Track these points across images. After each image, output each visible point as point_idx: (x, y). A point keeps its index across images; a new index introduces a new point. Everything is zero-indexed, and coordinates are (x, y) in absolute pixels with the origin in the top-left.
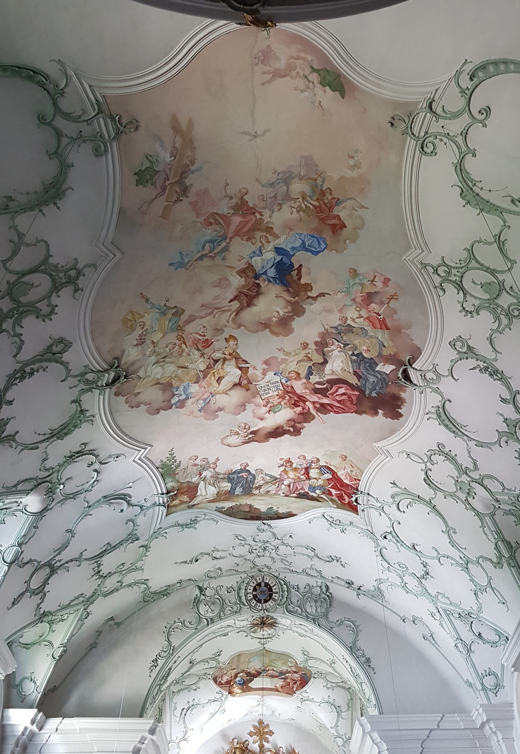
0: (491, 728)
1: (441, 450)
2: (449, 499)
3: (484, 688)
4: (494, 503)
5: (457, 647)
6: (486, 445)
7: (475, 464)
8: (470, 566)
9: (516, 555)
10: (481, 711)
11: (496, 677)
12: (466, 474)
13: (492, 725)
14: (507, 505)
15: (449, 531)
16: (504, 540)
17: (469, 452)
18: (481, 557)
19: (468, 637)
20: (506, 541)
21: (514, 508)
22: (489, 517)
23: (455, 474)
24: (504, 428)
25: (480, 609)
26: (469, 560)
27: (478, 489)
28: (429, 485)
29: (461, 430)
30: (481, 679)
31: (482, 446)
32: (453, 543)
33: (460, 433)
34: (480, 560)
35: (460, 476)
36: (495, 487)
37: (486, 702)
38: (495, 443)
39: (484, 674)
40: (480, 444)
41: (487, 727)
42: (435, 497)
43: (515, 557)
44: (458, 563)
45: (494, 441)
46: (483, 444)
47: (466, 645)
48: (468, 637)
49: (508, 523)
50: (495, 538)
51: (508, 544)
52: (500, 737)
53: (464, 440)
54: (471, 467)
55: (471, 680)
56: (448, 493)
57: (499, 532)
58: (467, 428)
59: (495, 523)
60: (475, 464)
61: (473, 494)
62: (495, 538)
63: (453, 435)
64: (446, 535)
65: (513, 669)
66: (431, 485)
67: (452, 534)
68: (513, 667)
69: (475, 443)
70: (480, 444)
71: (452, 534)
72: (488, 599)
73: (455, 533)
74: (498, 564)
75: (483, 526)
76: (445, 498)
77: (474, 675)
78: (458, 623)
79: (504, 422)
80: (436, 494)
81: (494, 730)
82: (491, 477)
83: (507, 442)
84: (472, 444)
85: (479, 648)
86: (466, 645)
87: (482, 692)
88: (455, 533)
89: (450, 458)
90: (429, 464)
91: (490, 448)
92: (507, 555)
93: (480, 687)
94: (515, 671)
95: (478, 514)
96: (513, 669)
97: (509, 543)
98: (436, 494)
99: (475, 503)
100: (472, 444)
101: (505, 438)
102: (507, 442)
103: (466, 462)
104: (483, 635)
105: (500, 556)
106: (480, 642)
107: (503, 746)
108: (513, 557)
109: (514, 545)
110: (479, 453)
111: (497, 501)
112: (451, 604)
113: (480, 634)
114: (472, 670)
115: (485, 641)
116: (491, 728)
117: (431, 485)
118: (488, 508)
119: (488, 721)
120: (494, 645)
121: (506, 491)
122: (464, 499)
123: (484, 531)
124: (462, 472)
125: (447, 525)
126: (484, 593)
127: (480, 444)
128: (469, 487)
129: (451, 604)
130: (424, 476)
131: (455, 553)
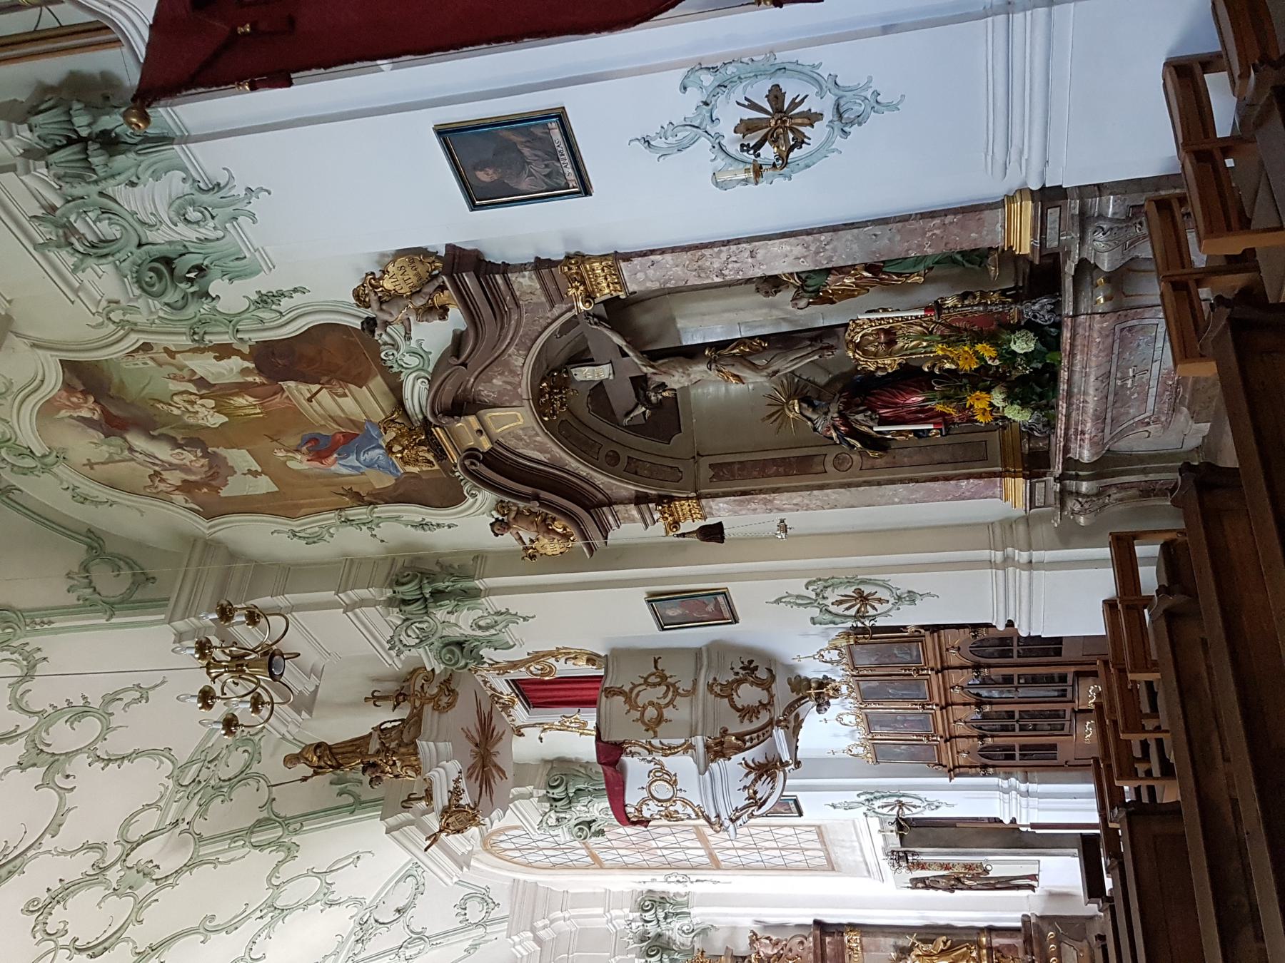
0: (545, 927)
1: (38, 910)
2: (145, 915)
3: (482, 924)
4: (177, 830)
5: (411, 958)
6: (59, 816)
7: (91, 848)
8: (279, 904)
9: (282, 815)
10: (516, 939)
11: (469, 897)
12: (105, 869)
13: (540, 924)
14: (190, 808)
15: (207, 929)
16: (251, 830)
17: (64, 853)
18: (269, 879)
19: (397, 935)
20: (254, 826)
21: (199, 796)
22: (201, 847)
23: (99, 891)
24: (36, 774)
25: (358, 902)
26: (269, 902)
27: (142, 854)
28: (106, 949)
29: (11, 857)
30: (467, 926)
31: (60, 825)
32: (231, 927)
33: (18, 862)
34: (275, 882)
35: (107, 884)
36: (150, 820)
37: (505, 926)
38: (61, 798)
39: (462, 918)
40: (54, 828)
41: (541, 933)
42: (134, 942)
43: (286, 818)
44: (269, 925)
45: (57, 799)
46: (57, 822)
47: (410, 942)
48: (397, 935)
49: (222, 815)
50: (243, 846)
51: (259, 824)
52: (558, 914)
53: (32, 858)
54: (94, 856)
55: (467, 945)
56: (134, 915)
57: (234, 836)
58: (11, 846)
59: (215, 839)
60: (91, 848)
61: (150, 865)
62: (243, 846)
63: (16, 876)
64: (213, 936)
65: (465, 869)
66: (106, 945)
67: (214, 923)
68: (462, 869)
69: (48, 836)
70: (54, 828)
71: (214, 923)
72: (344, 884)
73: (213, 917)
74: (291, 851)
75: (215, 863)
76: (141, 922)
77: (460, 937)
78: (372, 947)
79: (23, 770)
80: (127, 940)
81: (547, 922)
82: (127, 823)
83: (68, 776)
84: (48, 842)
85: (421, 918)
86: (410, 942)
87: (489, 929)
88: (213, 917)
89: (61, 895)
90: (62, 941)
91: (69, 810)
92: (279, 832)
93: (481, 931)
94: (468, 866)
95: (189, 866)
96: (465, 869)
97: (259, 824)
98: (127, 940)
99: (168, 866)
100: (48, 842)
101: (59, 779)
102: (68, 776)
103: (84, 863)
104: (401, 905)
105: (278, 844)
106: (410, 912)
107: (574, 912)
108: (284, 822)
109: (264, 814)
110: (70, 835)
111: (176, 823)
112: (336, 953)
113: (398, 911)
114: (453, 939)
115: (411, 904)
116: (545, 927)
117: (106, 945)
118: (184, 844)
119: (533, 930)
120: (421, 888)
121: (161, 804)
122: (153, 886)
123: (226, 863)
124: (101, 877)
125: (194, 931)
126: (333, 888)
127: (54, 826)
128: (134, 871)
129: (336, 953)
130: (84, 956)
131: (250, 928)
